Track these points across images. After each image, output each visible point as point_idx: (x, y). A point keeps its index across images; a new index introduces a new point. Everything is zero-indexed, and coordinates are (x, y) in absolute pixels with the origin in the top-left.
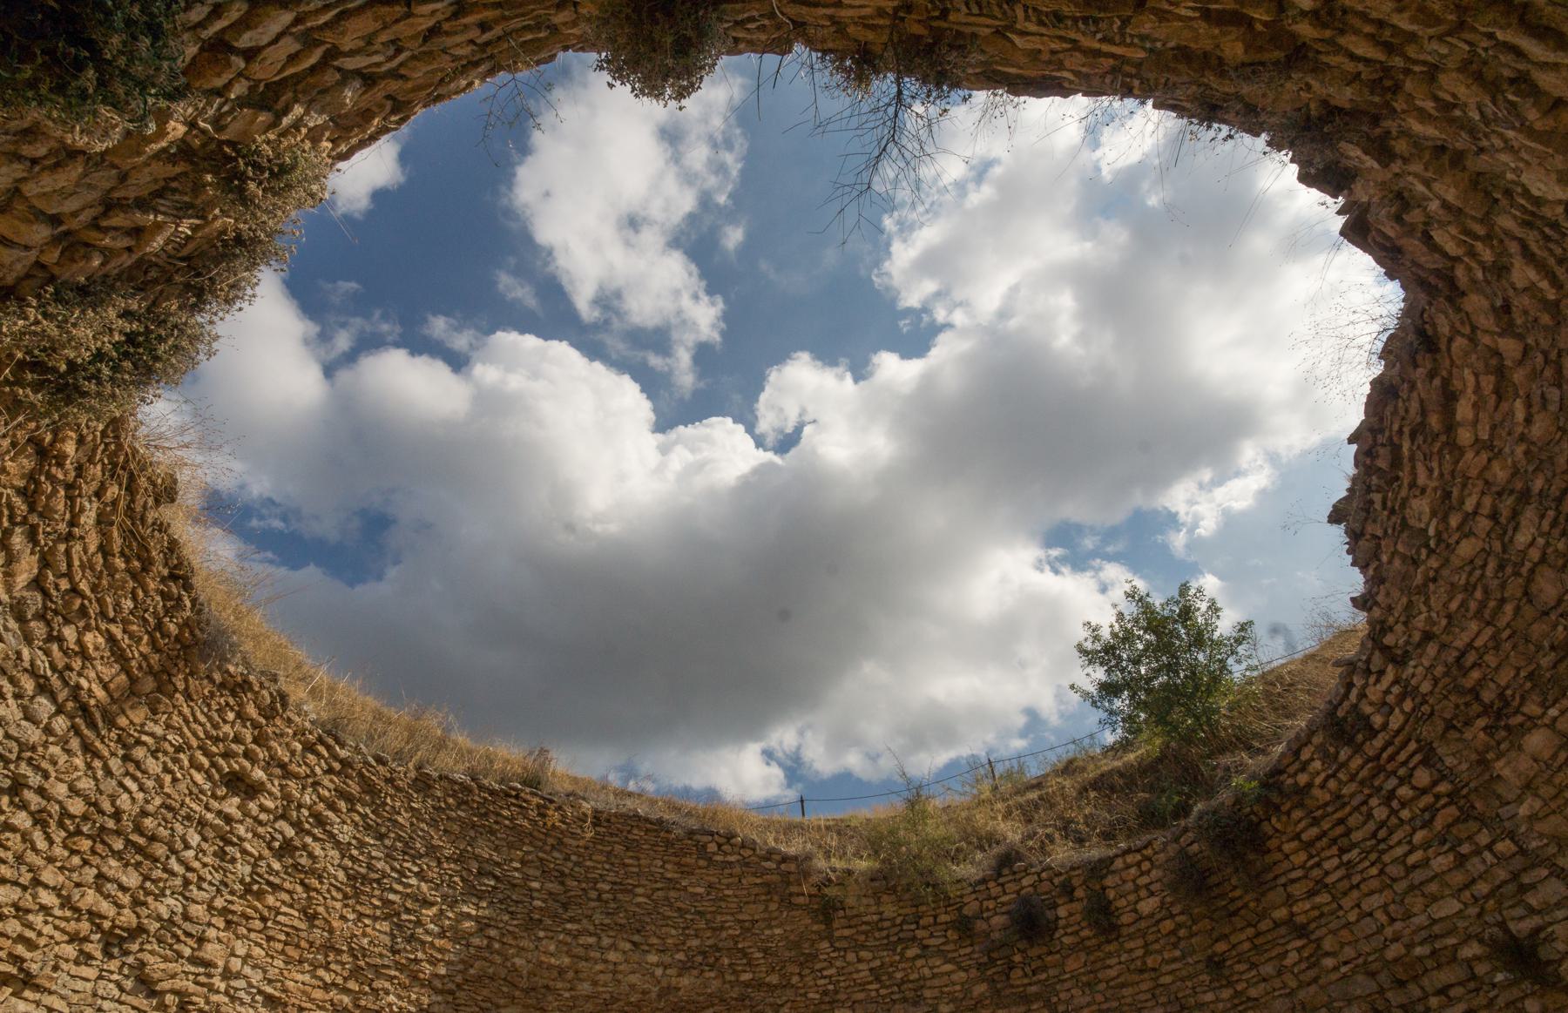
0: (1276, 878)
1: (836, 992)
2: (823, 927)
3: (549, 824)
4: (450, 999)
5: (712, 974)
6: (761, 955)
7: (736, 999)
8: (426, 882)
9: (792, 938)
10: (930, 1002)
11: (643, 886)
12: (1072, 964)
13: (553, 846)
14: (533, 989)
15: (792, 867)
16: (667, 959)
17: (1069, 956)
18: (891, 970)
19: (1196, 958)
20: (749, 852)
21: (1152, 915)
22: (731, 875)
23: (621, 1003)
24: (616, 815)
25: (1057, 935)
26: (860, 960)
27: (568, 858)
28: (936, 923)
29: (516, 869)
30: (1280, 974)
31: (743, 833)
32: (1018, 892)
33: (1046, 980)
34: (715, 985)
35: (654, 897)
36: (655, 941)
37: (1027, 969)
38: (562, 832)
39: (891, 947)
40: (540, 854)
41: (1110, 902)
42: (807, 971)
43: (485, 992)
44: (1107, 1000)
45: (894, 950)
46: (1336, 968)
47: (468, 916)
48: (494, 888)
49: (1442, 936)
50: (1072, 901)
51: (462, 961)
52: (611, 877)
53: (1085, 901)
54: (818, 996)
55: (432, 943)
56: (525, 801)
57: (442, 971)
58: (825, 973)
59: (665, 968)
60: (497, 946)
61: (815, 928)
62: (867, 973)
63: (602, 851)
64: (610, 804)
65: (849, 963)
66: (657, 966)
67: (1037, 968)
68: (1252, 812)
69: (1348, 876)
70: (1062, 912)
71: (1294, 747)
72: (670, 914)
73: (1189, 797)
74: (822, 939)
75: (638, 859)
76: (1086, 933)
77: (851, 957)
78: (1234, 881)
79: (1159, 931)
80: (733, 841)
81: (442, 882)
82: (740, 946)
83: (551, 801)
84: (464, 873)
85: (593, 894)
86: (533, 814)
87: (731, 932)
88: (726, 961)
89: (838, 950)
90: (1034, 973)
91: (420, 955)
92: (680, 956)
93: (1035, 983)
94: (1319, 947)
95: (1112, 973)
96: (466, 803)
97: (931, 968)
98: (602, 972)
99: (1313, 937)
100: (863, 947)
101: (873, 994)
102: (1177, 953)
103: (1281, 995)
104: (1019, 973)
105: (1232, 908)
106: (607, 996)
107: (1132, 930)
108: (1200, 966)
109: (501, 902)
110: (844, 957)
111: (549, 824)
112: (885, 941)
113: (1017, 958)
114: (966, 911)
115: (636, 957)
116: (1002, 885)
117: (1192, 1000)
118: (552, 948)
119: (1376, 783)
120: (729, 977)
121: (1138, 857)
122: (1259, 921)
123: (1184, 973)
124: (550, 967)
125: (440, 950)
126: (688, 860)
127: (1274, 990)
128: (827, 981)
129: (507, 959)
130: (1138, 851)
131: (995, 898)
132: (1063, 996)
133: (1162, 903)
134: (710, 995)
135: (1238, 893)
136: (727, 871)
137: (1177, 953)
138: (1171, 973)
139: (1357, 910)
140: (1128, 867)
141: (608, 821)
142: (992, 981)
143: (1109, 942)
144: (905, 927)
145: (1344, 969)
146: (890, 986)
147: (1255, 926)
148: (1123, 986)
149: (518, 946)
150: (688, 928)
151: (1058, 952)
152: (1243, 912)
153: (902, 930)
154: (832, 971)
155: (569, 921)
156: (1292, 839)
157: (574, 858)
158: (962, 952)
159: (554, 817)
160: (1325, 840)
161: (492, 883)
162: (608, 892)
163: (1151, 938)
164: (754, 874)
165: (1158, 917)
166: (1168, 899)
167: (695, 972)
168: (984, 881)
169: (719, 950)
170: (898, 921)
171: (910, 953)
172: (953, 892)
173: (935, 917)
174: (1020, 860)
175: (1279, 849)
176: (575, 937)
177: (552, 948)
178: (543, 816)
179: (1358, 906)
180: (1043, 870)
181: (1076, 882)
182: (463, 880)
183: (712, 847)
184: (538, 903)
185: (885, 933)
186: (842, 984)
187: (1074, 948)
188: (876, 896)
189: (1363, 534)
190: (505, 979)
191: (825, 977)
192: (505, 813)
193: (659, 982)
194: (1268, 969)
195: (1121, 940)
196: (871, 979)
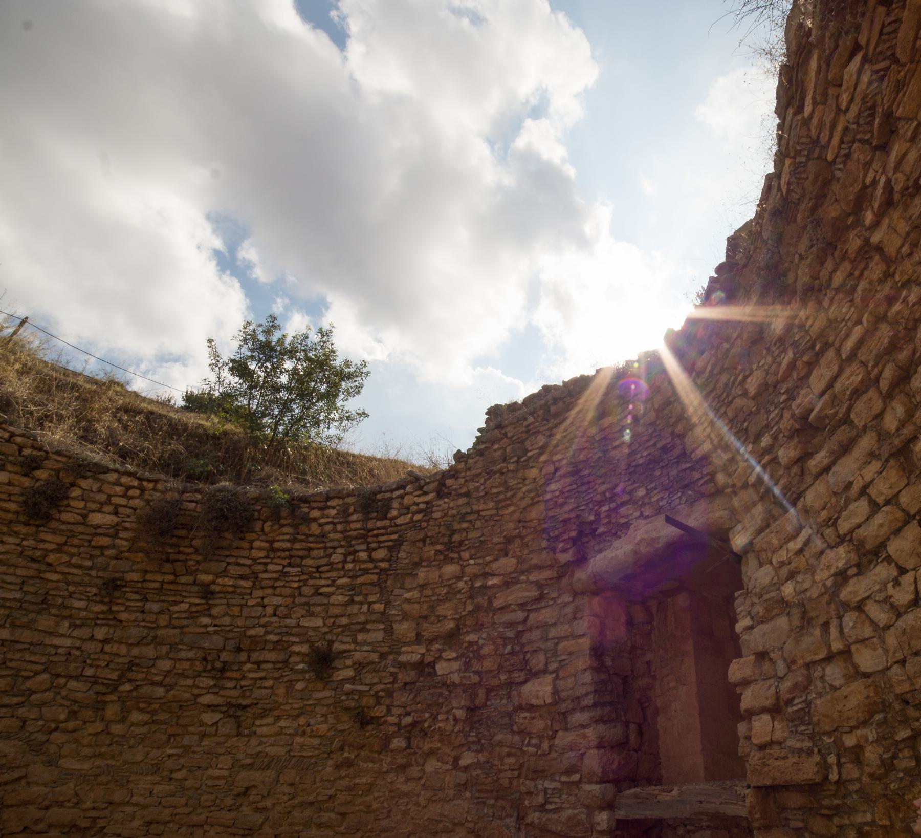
0: (227, 556)
19: (101, 574)
21: (98, 527)
30: (160, 613)
41: (67, 498)
46: (206, 626)
49: (293, 635)
50: (25, 475)
68: (259, 511)
69: (276, 580)
71: (332, 495)
73: (221, 473)
79: (90, 541)
94: (209, 609)
99: (211, 602)
103: (145, 627)
105: (172, 557)
107: (64, 527)
108: (99, 581)
117: (60, 601)
119: (353, 542)
121: (136, 483)
122: (183, 575)
123: (77, 579)
127: (144, 621)
130: (140, 479)
133: (117, 524)
135: (191, 550)
137: (88, 563)
138: (63, 573)
139: (259, 600)
140: (117, 483)
143: (26, 524)
145: (210, 629)
147: (176, 576)
156: (266, 541)
160: (287, 553)
163: (75, 541)
165: (99, 531)
166: (127, 525)
175: (251, 542)
179: (263, 598)
189: (503, 428)
194: (155, 607)
195: (42, 529)
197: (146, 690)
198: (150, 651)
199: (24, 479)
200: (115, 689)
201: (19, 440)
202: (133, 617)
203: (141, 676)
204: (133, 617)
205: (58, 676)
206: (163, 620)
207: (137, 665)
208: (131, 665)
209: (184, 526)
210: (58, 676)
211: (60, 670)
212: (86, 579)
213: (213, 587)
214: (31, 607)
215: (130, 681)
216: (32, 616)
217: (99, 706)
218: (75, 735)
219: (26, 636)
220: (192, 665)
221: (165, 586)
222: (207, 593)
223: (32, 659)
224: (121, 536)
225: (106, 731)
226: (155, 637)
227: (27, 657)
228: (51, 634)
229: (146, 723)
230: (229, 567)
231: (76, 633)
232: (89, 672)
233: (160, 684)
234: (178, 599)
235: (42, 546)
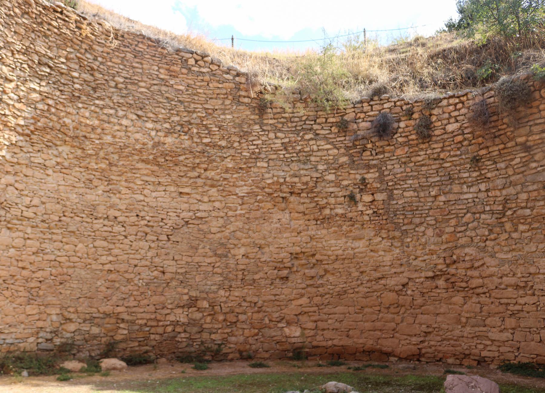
0: (527, 122)
1: (260, 153)
2: (257, 117)
3: (84, 34)
4: (28, 139)
5: (186, 137)
6: (217, 129)
7: (199, 152)
8: (6, 66)
9: (237, 121)
10: (314, 163)
11: (145, 82)
12: (399, 152)
13: (86, 50)
14: (77, 137)
15: (243, 80)
16: (158, 127)
17: (398, 148)
18: (294, 144)
19: (467, 156)
20: (217, 68)
22: (203, 80)
23: (130, 149)
24: (128, 33)
25: (396, 136)
26: (276, 138)
27: (95, 59)
28: (326, 122)
29: (63, 63)
30: (507, 168)
31: (213, 55)
32: (380, 111)
33: (382, 158)
34: (187, 143)
35: (151, 89)
36: (151, 115)
37: (374, 152)
38: (92, 41)
39: (297, 132)
40: (78, 55)
41: (432, 123)
42: (244, 141)
43: (48, 137)
44: (412, 171)
45: (298, 135)
46: (536, 168)
47: (34, 90)
48: (50, 74)
50: (410, 119)
51: (33, 118)
52: (124, 74)
53: (418, 120)
54: (248, 154)
55: (13, 105)
56: (67, 16)
57: (22, 122)
58: (255, 143)
59: (157, 131)
60: (53, 110)
61: (252, 117)
62: (280, 145)
63: (118, 57)
64: (125, 27)
65: (269, 139)
66: (152, 130)
67: (379, 152)
68: (533, 86)
70: (402, 125)
72: (161, 100)
74: (256, 124)
75: (142, 64)
76: (414, 137)
77: (272, 135)
78: (505, 120)
79: (453, 141)
80: (206, 59)
81: (16, 67)
82: (204, 123)
83: (85, 19)
84: (30, 63)
85: (113, 84)
86: (73, 26)
87: (199, 114)
88: (195, 131)
89: (264, 130)
90: (376, 154)
91: (7, 112)
92: (167, 125)
93: (376, 159)
94: (533, 157)
95: (419, 159)
96: (27, 13)
97: (318, 146)
98: (118, 130)
99: (532, 153)
100: (280, 131)
101: (282, 156)
102: (459, 153)
103: (502, 178)
104: (369, 153)
105: (497, 134)
106: (122, 144)
107: (439, 138)
108: (468, 160)
109: (54, 83)
110: (267, 135)
111: (84, 34)
112: (294, 129)
113: (369, 146)
114: (346, 118)
115: (139, 123)
116: (372, 106)
117: (457, 176)
118: (87, 114)
120: (195, 140)
122: (508, 142)
123: (458, 163)
124: (86, 125)
125: (19, 110)
126: (175, 68)
127: (500, 175)
128: (255, 147)
129: (60, 119)
131: (365, 113)
132: (389, 167)
133: (461, 127)
134: (184, 149)
135: (505, 126)
136: (200, 78)
137: (459, 153)
138: (451, 162)
140: (449, 105)
141: (123, 36)
142: (351, 156)
143: (423, 143)
144: (307, 122)
145: (539, 169)
146: (292, 153)
147: (505, 144)
148: (423, 165)
149: (66, 112)
150: (172, 110)
151: (393, 145)
152: (502, 136)
153: (305, 124)
154: (260, 142)
155: (97, 99)
157: (100, 59)
158: (338, 139)
159: (87, 30)
161: (48, 70)
162: (122, 83)
163: (447, 143)
164: (218, 82)
165: (455, 134)
166: (465, 125)
167: (176, 135)
168: (361, 102)
169: (191, 124)
170: (304, 118)
171: (307, 137)
172: (342, 105)
173: (327, 119)
174: (386, 93)
175: (538, 107)
176: (101, 109)
177: (87, 114)
178: (80, 28)
180: (398, 101)
181: (415, 109)
182: (29, 67)
183: (192, 62)
184: (77, 86)
185: (294, 124)
186: (264, 150)
187: (403, 144)
188: (294, 103)
190: (59, 130)
191: (254, 145)
192: (54, 23)
193: (153, 139)
194: (503, 165)
195: (430, 143)
196: (282, 148)
197: (520, 212)
198: (511, 191)
199: (411, 122)
200: (504, 215)
201: (398, 103)
202: (494, 174)
203: (514, 205)
204: (494, 174)
205: (474, 213)
206: (510, 171)
207: (509, 200)
208: (506, 200)
209: (494, 113)
210: (475, 213)
211: (474, 210)
212: (462, 161)
213: (529, 144)
214: (446, 183)
215: (510, 209)
216: (449, 187)
217: (502, 225)
218: (497, 241)
219: (452, 197)
220: (539, 193)
221: (502, 152)
222: (526, 148)
223: (460, 207)
224: (465, 132)
225: (510, 237)
226: (511, 182)
227: (457, 207)
228: (461, 193)
229: (529, 230)
230: (532, 128)
231: (472, 190)
232: (488, 208)
233: (526, 207)
234: (512, 157)
235: (435, 151)
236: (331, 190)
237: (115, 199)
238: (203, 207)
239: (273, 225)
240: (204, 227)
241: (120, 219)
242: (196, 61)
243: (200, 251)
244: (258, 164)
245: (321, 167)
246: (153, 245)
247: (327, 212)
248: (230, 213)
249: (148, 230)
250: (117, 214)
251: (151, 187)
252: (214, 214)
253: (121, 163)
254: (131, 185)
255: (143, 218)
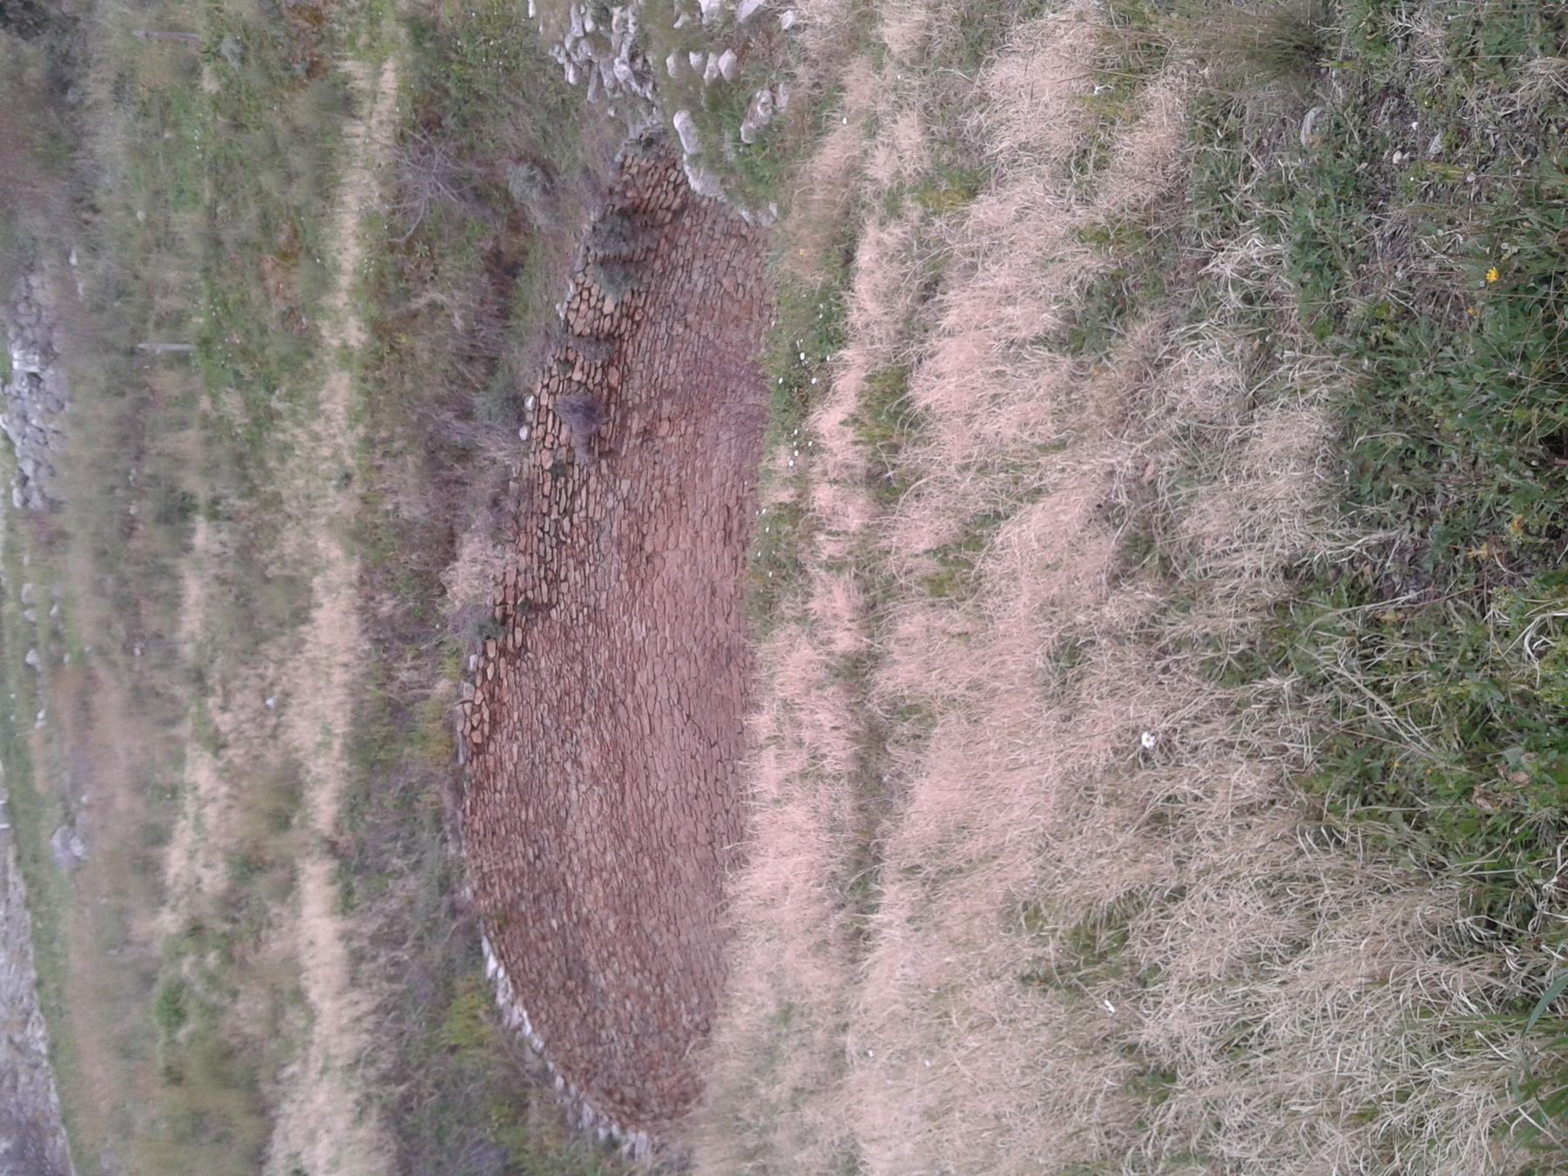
16: (573, 780)
26: (566, 579)
36: (561, 794)
92: (568, 766)
100: (557, 575)
114: (548, 465)
154: (573, 607)
236: (642, 485)
237: (682, 837)
238: (663, 694)
239: (687, 577)
240: (692, 686)
241: (707, 823)
242: (473, 728)
243: (725, 692)
244: (603, 606)
245: (610, 504)
246: (729, 768)
247: (671, 491)
248: (669, 647)
249: (710, 779)
250: (701, 829)
251: (653, 779)
252: (671, 674)
253: (635, 835)
254: (657, 812)
255: (698, 788)
